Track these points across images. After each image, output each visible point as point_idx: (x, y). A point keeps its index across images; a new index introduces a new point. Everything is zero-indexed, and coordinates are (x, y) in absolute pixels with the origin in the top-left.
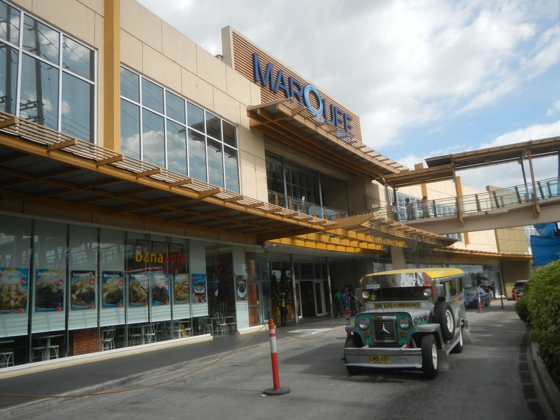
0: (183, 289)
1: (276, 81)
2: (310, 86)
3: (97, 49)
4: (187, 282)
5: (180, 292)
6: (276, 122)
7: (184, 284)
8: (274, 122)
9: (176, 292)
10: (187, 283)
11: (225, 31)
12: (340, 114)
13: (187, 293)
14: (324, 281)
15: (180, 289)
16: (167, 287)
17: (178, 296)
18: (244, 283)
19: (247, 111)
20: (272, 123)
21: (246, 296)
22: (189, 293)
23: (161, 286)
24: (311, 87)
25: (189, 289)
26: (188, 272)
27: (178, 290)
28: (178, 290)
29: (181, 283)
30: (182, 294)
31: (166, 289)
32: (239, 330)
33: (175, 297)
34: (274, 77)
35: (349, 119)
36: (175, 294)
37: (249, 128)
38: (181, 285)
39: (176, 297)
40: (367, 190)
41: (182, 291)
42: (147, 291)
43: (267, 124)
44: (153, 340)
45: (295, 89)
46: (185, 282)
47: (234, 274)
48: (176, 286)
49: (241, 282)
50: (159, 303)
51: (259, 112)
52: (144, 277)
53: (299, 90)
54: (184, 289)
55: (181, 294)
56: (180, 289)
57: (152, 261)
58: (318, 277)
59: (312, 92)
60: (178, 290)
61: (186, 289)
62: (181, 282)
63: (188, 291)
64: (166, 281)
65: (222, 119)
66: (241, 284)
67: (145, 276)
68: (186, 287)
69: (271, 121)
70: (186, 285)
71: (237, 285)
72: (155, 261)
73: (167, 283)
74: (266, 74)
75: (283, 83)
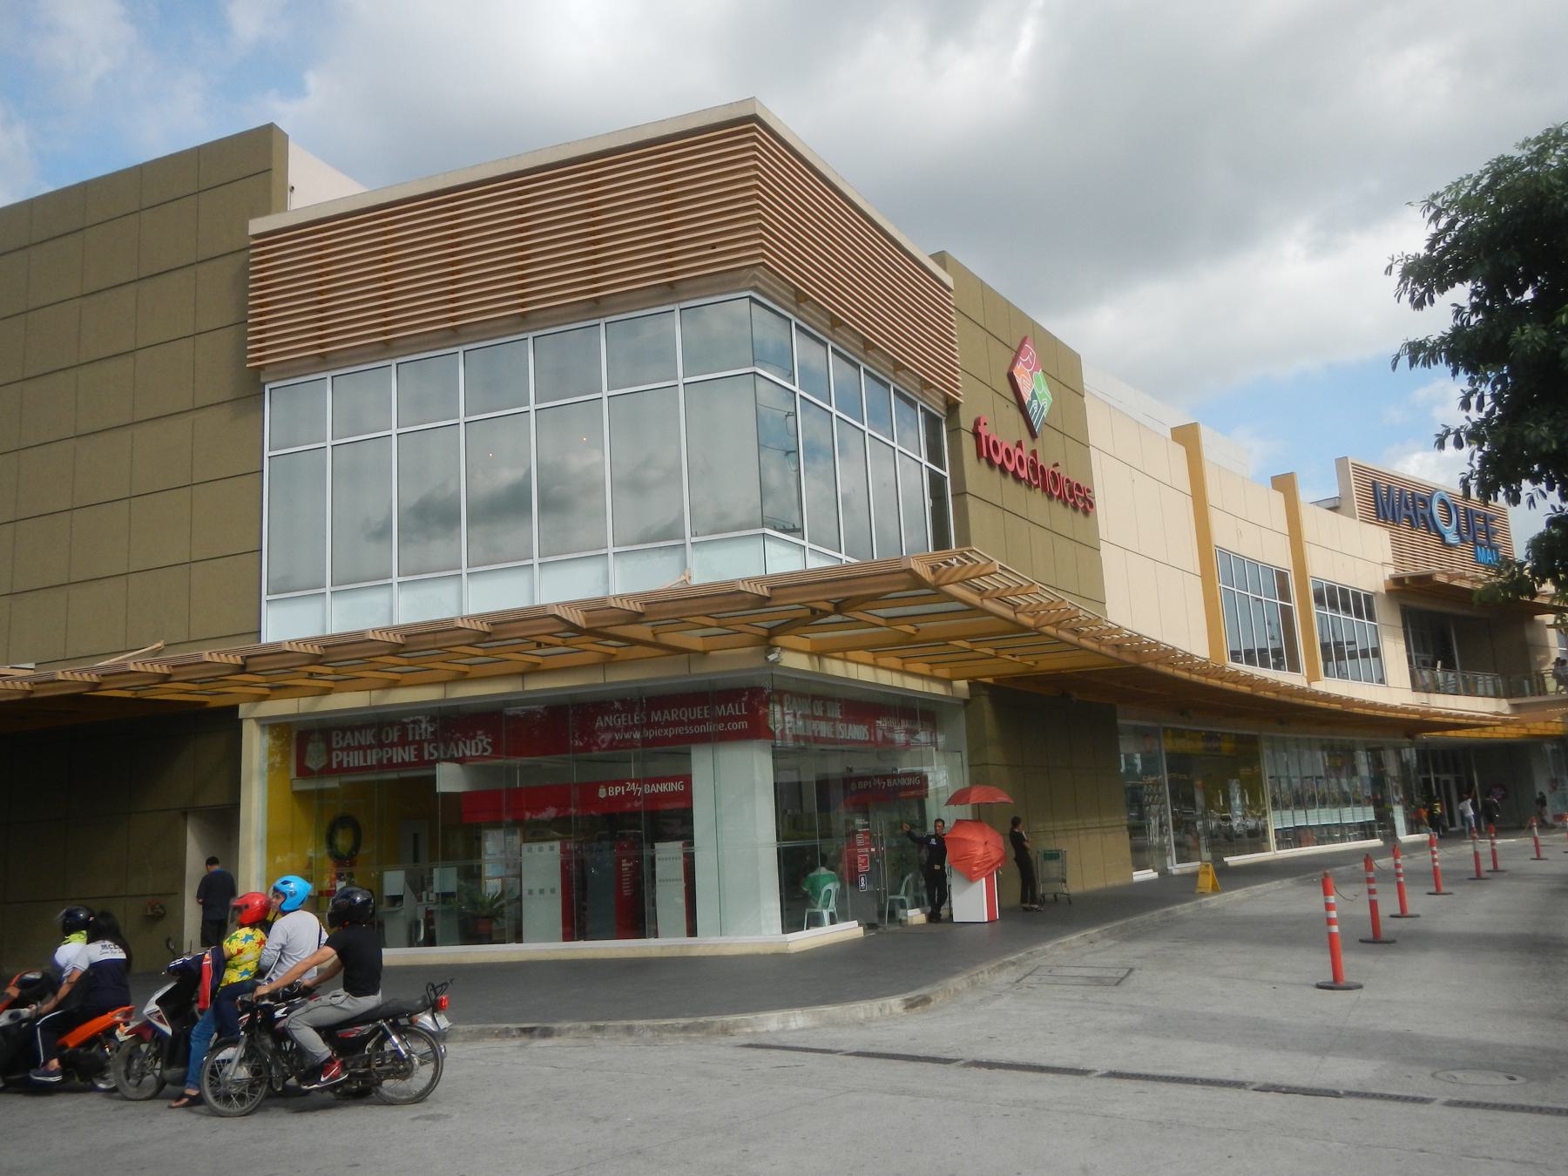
1: (1399, 506)
3: (1289, 571)
11: (1341, 463)
12: (1478, 516)
14: (1456, 778)
24: (1440, 495)
32: (1400, 838)
37: (1384, 592)
40: (1529, 634)
44: (1356, 839)
45: (1420, 506)
47: (1388, 776)
51: (1407, 582)
53: (1425, 504)
58: (1447, 771)
65: (1362, 593)
74: (1388, 503)
75: (1408, 508)
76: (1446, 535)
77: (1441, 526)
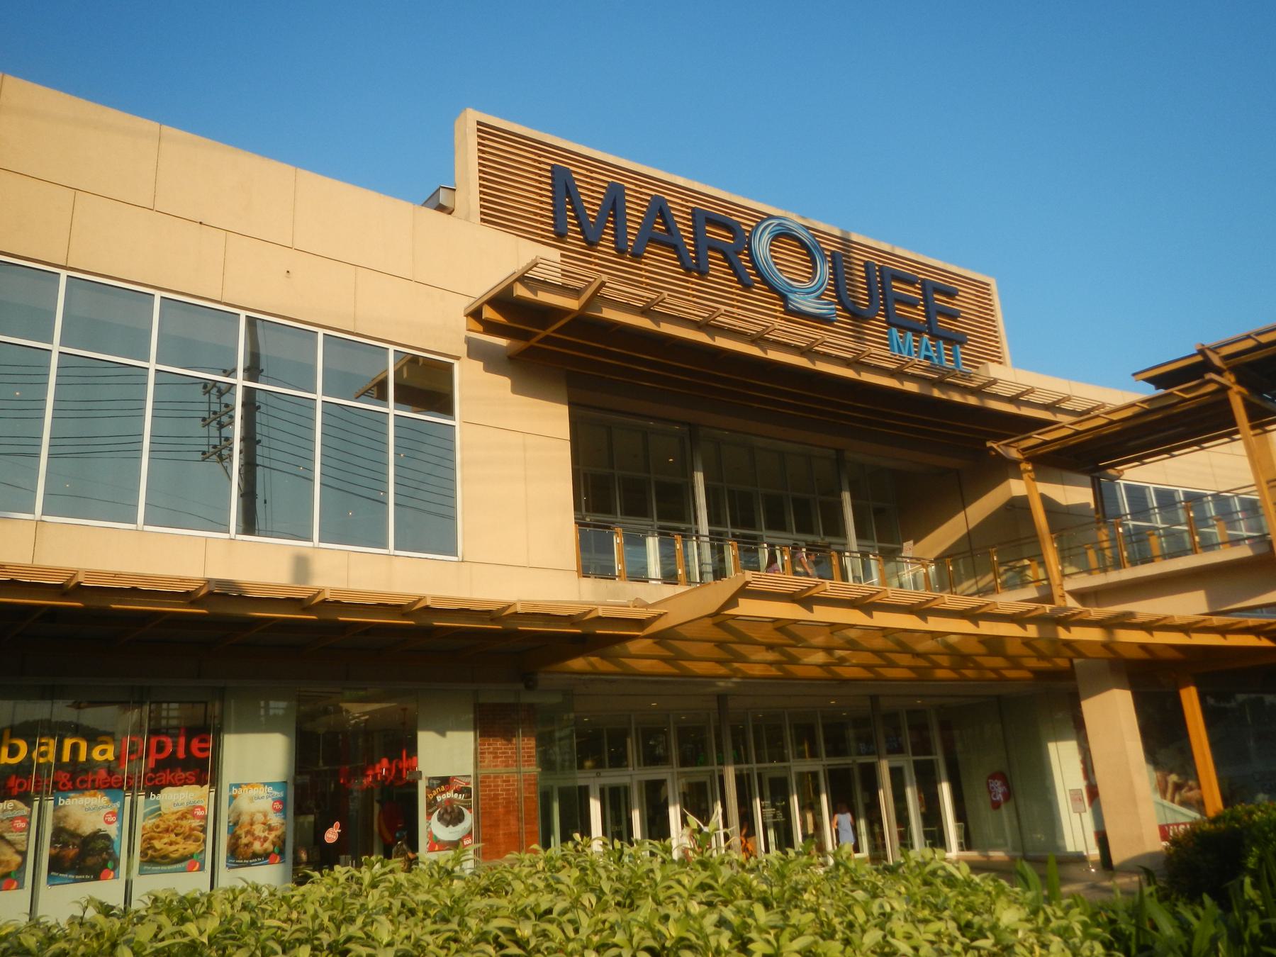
0: (178, 830)
2: (776, 222)
4: (202, 809)
5: (166, 840)
6: (554, 332)
7: (189, 816)
8: (549, 331)
9: (151, 838)
10: (199, 813)
13: (197, 840)
14: (916, 763)
15: (167, 830)
16: (112, 830)
17: (156, 850)
18: (461, 797)
19: (467, 316)
20: (548, 337)
21: (469, 834)
22: (204, 841)
23: (87, 829)
24: (779, 225)
25: (204, 830)
26: (215, 782)
27: (156, 835)
28: (156, 835)
29: (176, 813)
30: (177, 843)
31: (107, 837)
33: (144, 853)
34: (634, 213)
35: (951, 294)
36: (145, 846)
38: (174, 817)
39: (147, 854)
41: (177, 835)
42: (23, 849)
43: (539, 342)
46: (193, 810)
48: (150, 822)
49: (449, 795)
50: (73, 877)
52: (15, 808)
54: (187, 829)
55: (171, 844)
56: (167, 830)
57: (66, 757)
59: (784, 235)
60: (159, 832)
61: (192, 829)
62: (175, 809)
63: (201, 835)
64: (108, 814)
66: (450, 801)
67: (20, 805)
68: (196, 823)
69: (543, 334)
70: (194, 816)
71: (431, 804)
72: (82, 757)
73: (111, 819)
76: (791, 296)
77: (781, 279)
